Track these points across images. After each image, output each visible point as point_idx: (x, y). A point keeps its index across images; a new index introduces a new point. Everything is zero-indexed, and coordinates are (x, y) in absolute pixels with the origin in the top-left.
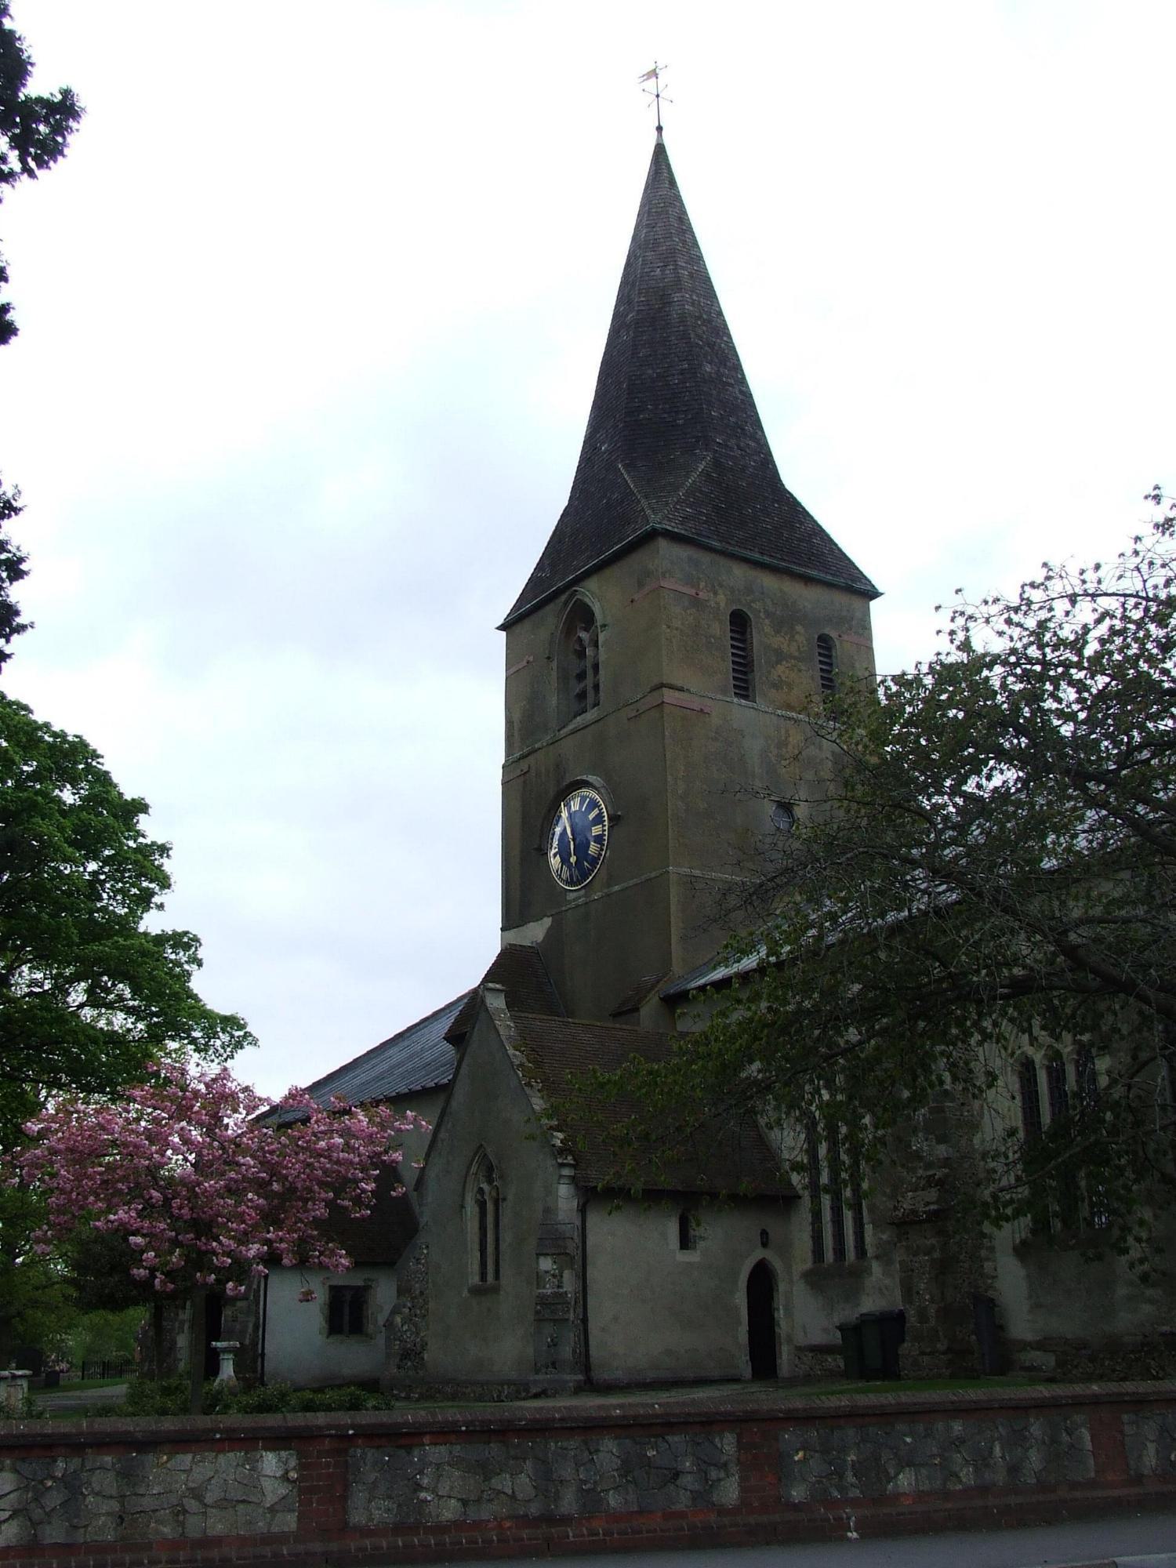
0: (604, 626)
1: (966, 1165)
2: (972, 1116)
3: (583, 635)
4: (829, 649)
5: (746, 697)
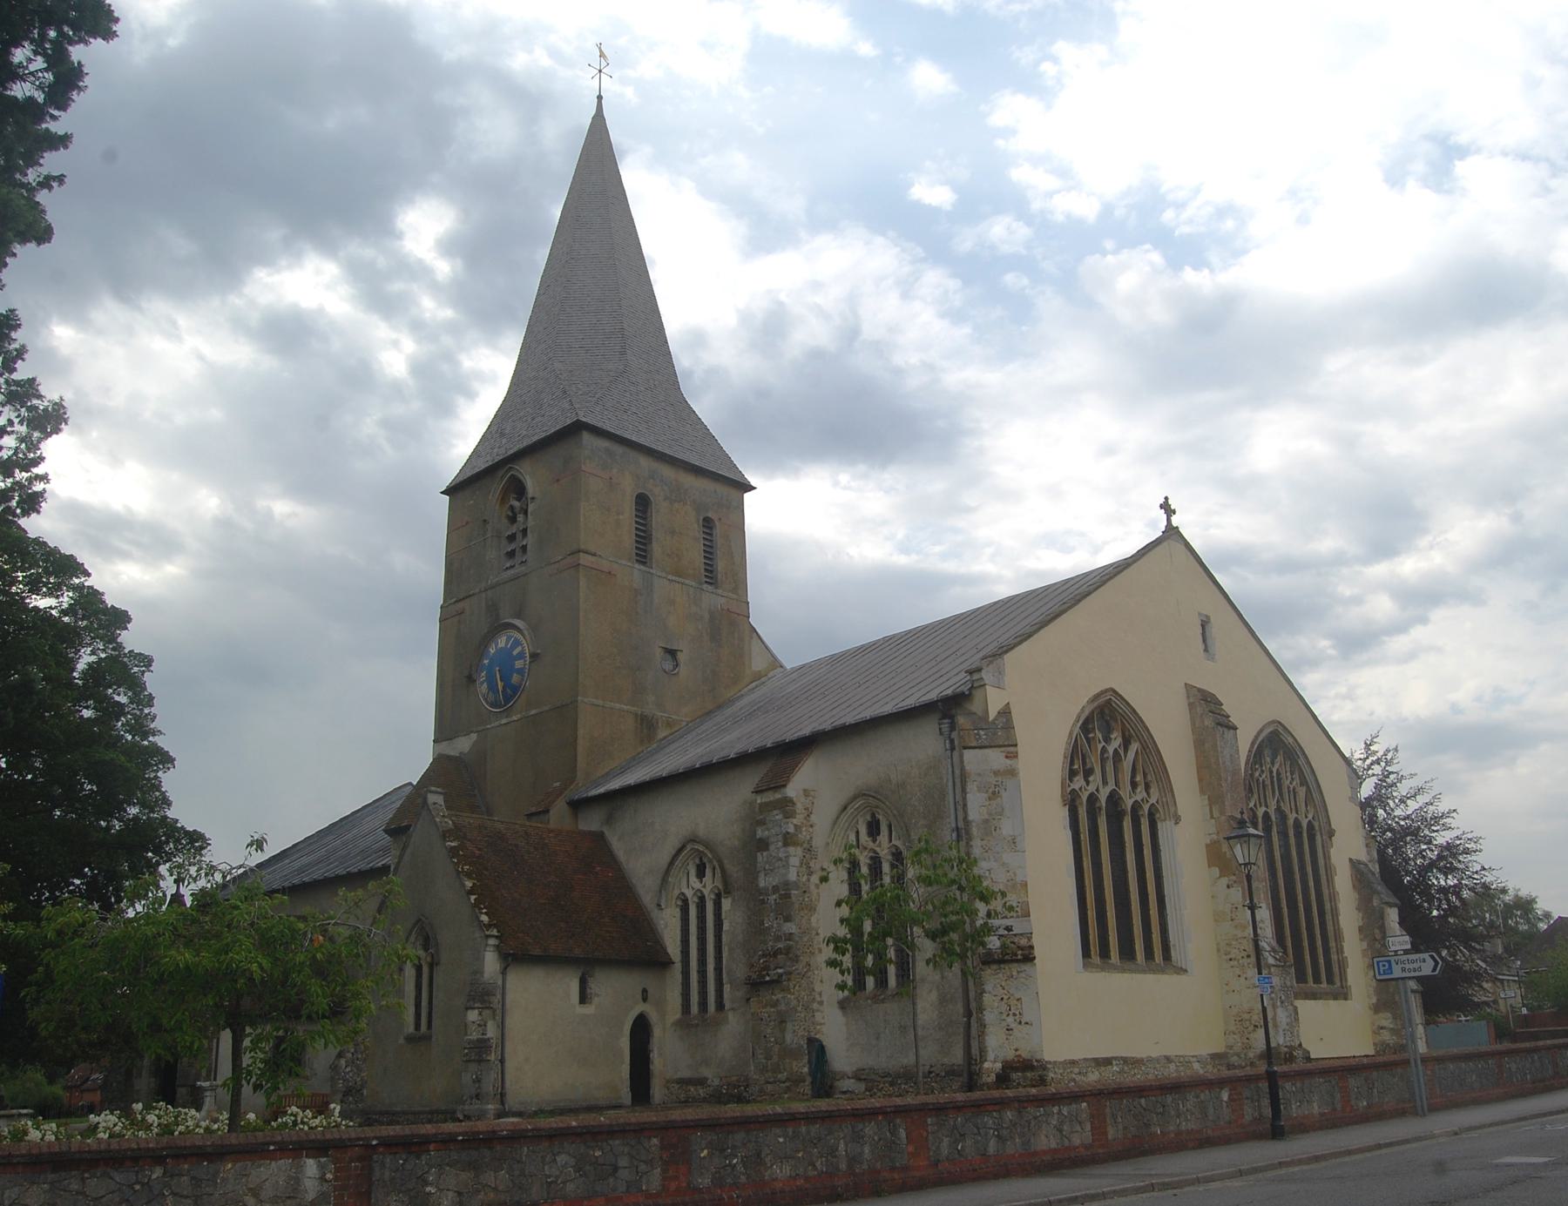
0: (533, 498)
1: (805, 939)
2: (811, 900)
4: (711, 528)
5: (644, 563)
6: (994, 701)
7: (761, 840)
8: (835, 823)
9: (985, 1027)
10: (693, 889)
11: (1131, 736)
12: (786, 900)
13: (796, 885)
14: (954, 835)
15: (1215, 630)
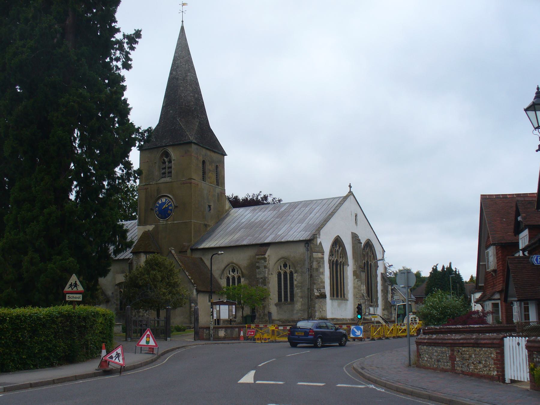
3: (165, 159)
6: (319, 241)
7: (258, 266)
8: (275, 264)
9: (316, 311)
10: (231, 275)
11: (340, 246)
12: (265, 281)
13: (267, 278)
14: (307, 270)
15: (358, 217)
